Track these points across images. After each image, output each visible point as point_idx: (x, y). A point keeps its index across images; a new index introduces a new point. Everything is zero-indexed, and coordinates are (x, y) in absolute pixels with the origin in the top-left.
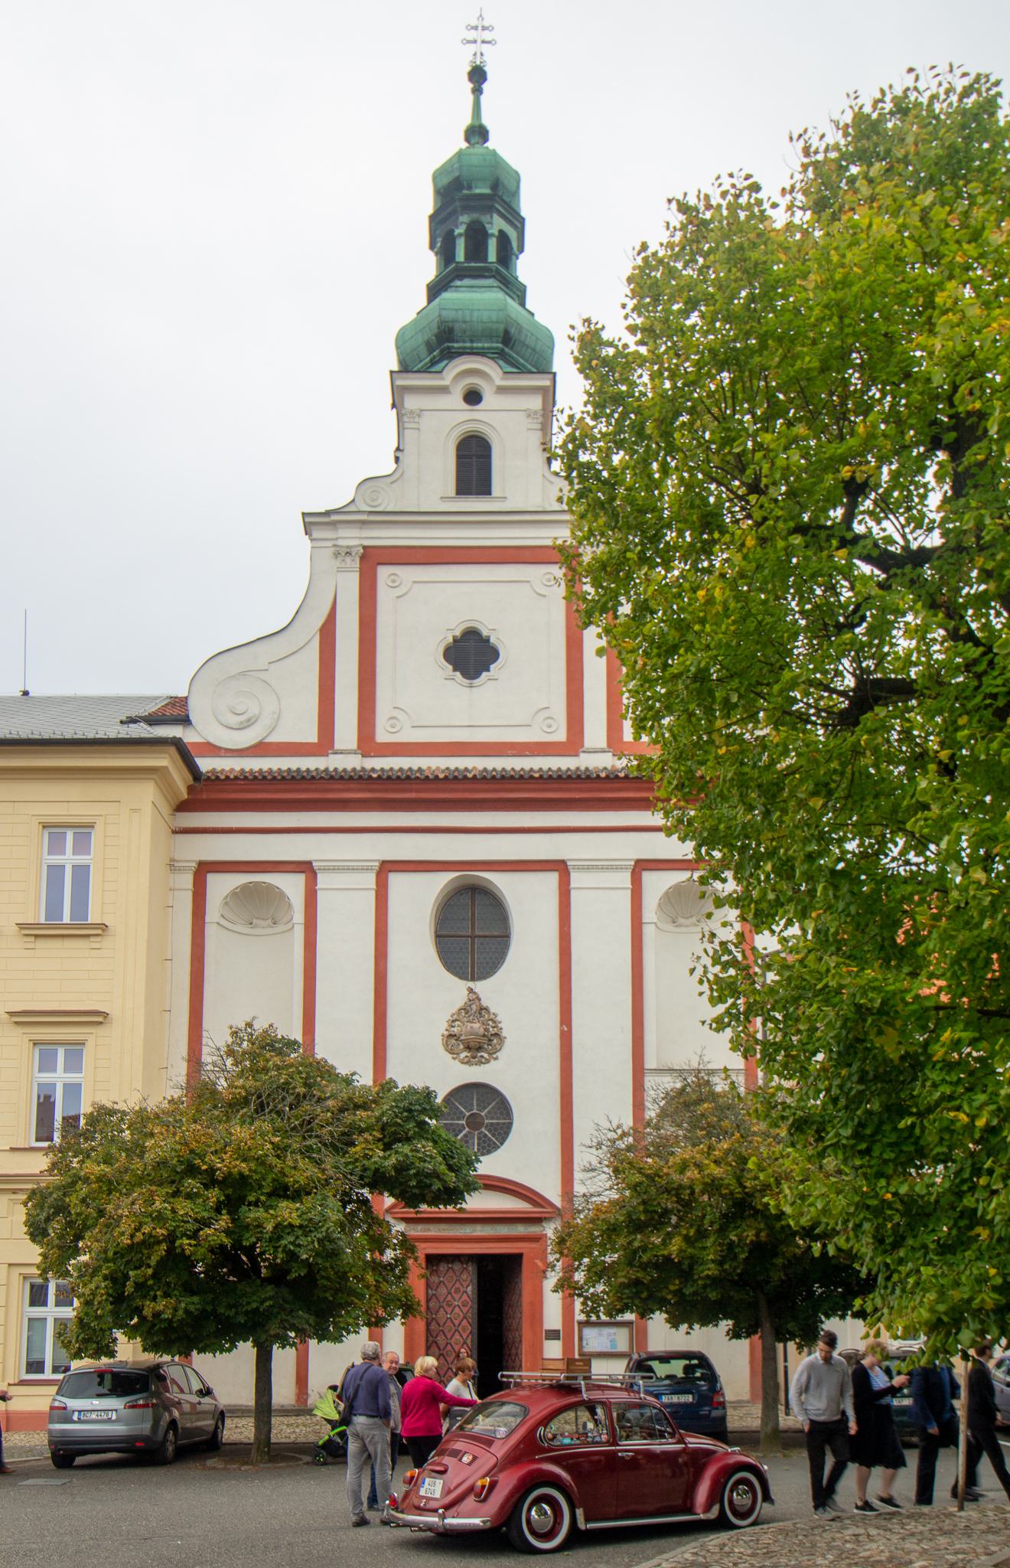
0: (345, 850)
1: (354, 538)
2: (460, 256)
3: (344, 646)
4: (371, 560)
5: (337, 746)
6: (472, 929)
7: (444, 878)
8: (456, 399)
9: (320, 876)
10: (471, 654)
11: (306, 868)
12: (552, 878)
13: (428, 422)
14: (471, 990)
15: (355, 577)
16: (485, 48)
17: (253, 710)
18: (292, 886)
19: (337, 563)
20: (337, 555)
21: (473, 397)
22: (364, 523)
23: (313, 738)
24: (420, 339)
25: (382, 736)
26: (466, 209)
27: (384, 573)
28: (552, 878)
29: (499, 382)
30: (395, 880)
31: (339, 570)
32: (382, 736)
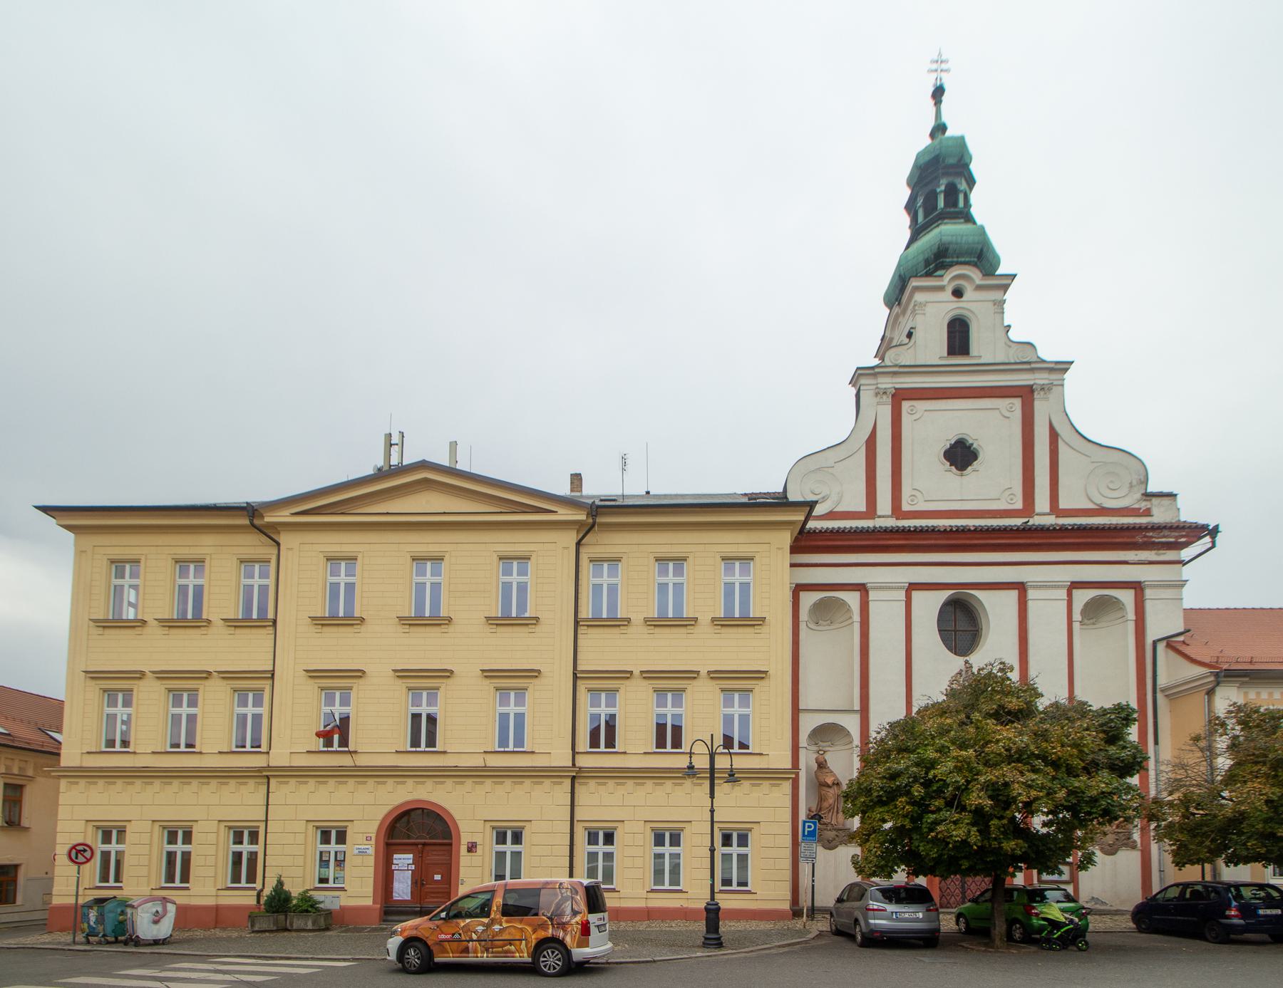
0: (886, 576)
1: (888, 383)
2: (941, 204)
3: (879, 453)
4: (899, 397)
5: (879, 513)
6: (961, 623)
7: (945, 595)
8: (947, 295)
9: (871, 593)
10: (961, 455)
11: (862, 588)
12: (1014, 594)
13: (930, 309)
14: (966, 662)
15: (889, 408)
16: (944, 75)
17: (825, 492)
18: (852, 599)
19: (878, 399)
20: (877, 394)
21: (958, 293)
22: (895, 373)
23: (863, 509)
24: (921, 258)
25: (906, 507)
26: (945, 174)
27: (906, 405)
28: (1014, 594)
29: (978, 282)
30: (916, 595)
31: (878, 404)
32: (906, 507)
